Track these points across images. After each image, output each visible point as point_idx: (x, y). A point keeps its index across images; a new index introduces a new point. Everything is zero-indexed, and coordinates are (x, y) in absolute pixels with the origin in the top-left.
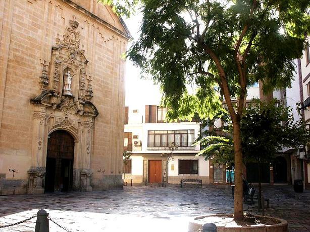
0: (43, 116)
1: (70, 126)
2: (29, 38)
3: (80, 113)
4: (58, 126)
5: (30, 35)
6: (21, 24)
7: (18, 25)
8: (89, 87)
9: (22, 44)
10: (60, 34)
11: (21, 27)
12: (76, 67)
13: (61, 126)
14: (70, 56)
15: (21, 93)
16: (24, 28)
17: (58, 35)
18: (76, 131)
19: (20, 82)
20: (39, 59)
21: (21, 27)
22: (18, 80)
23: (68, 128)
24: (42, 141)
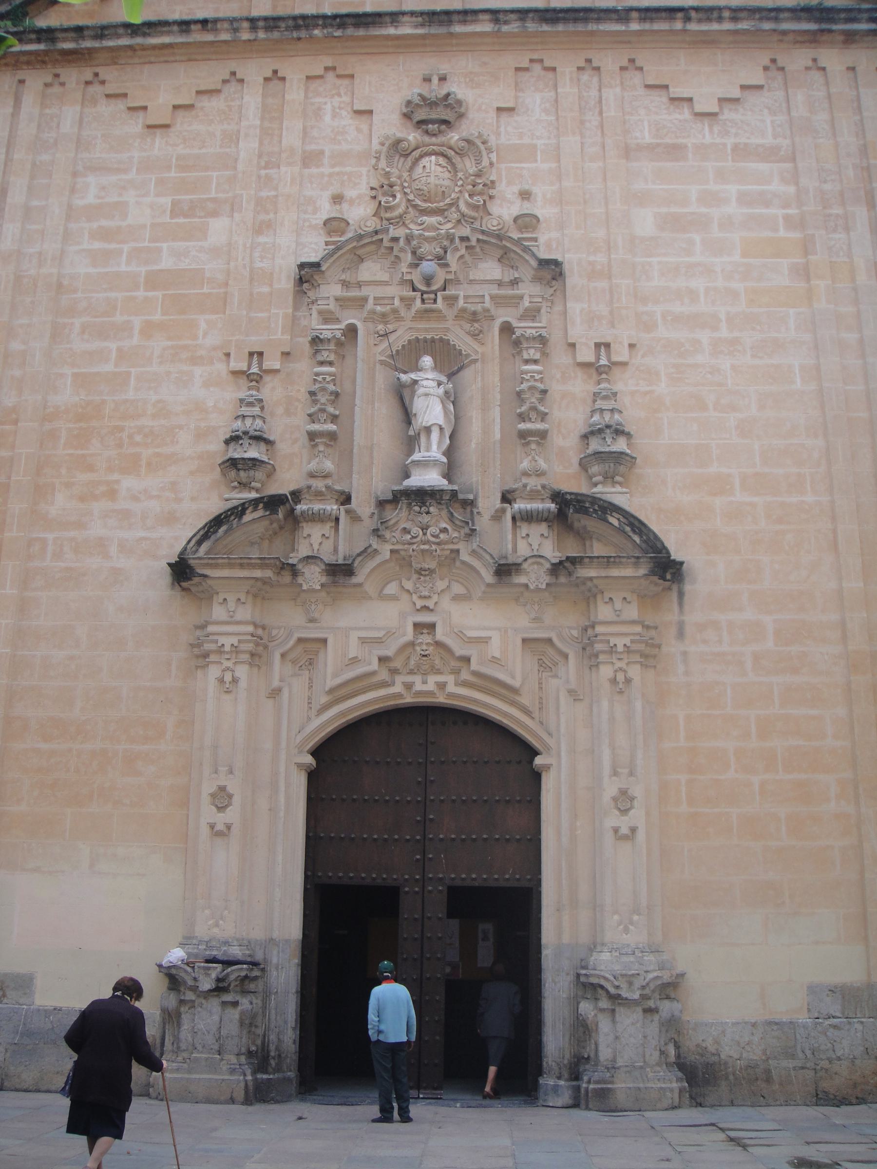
0: (222, 640)
1: (465, 675)
2: (153, 281)
3: (522, 579)
4: (361, 684)
5: (166, 263)
6: (105, 235)
7: (97, 245)
8: (600, 404)
9: (119, 318)
10: (351, 193)
11: (113, 246)
12: (474, 317)
13: (393, 684)
14: (416, 277)
15: (113, 550)
16: (126, 248)
17: (337, 199)
18: (525, 700)
19: (112, 494)
20: (220, 354)
21: (113, 246)
22: (103, 488)
23: (451, 688)
24: (233, 787)
